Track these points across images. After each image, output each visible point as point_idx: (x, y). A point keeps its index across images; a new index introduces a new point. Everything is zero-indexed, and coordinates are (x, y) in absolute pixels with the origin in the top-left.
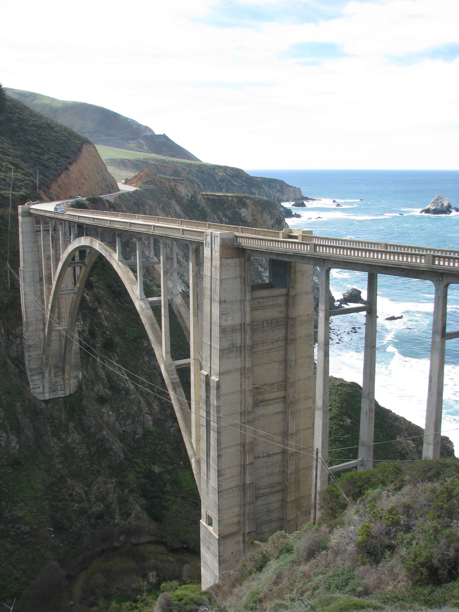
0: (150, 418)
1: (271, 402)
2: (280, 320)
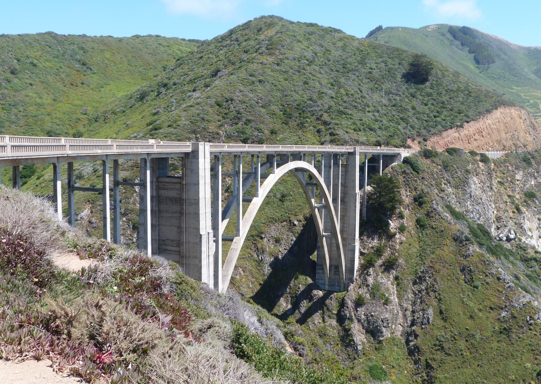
0: (401, 328)
1: (172, 252)
2: (178, 199)
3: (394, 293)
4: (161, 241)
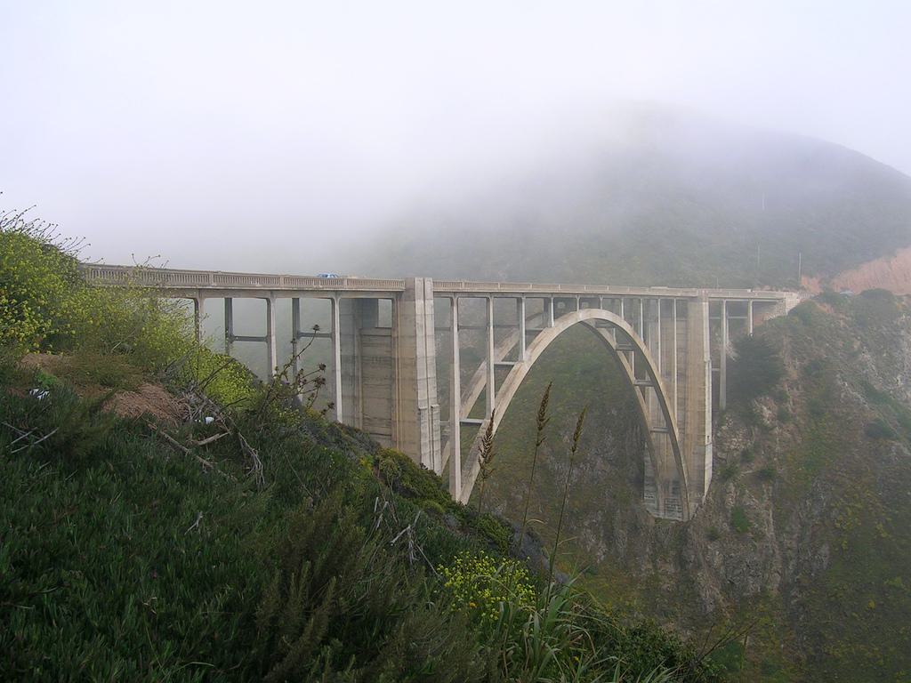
0: (779, 579)
3: (768, 522)
4: (367, 421)
